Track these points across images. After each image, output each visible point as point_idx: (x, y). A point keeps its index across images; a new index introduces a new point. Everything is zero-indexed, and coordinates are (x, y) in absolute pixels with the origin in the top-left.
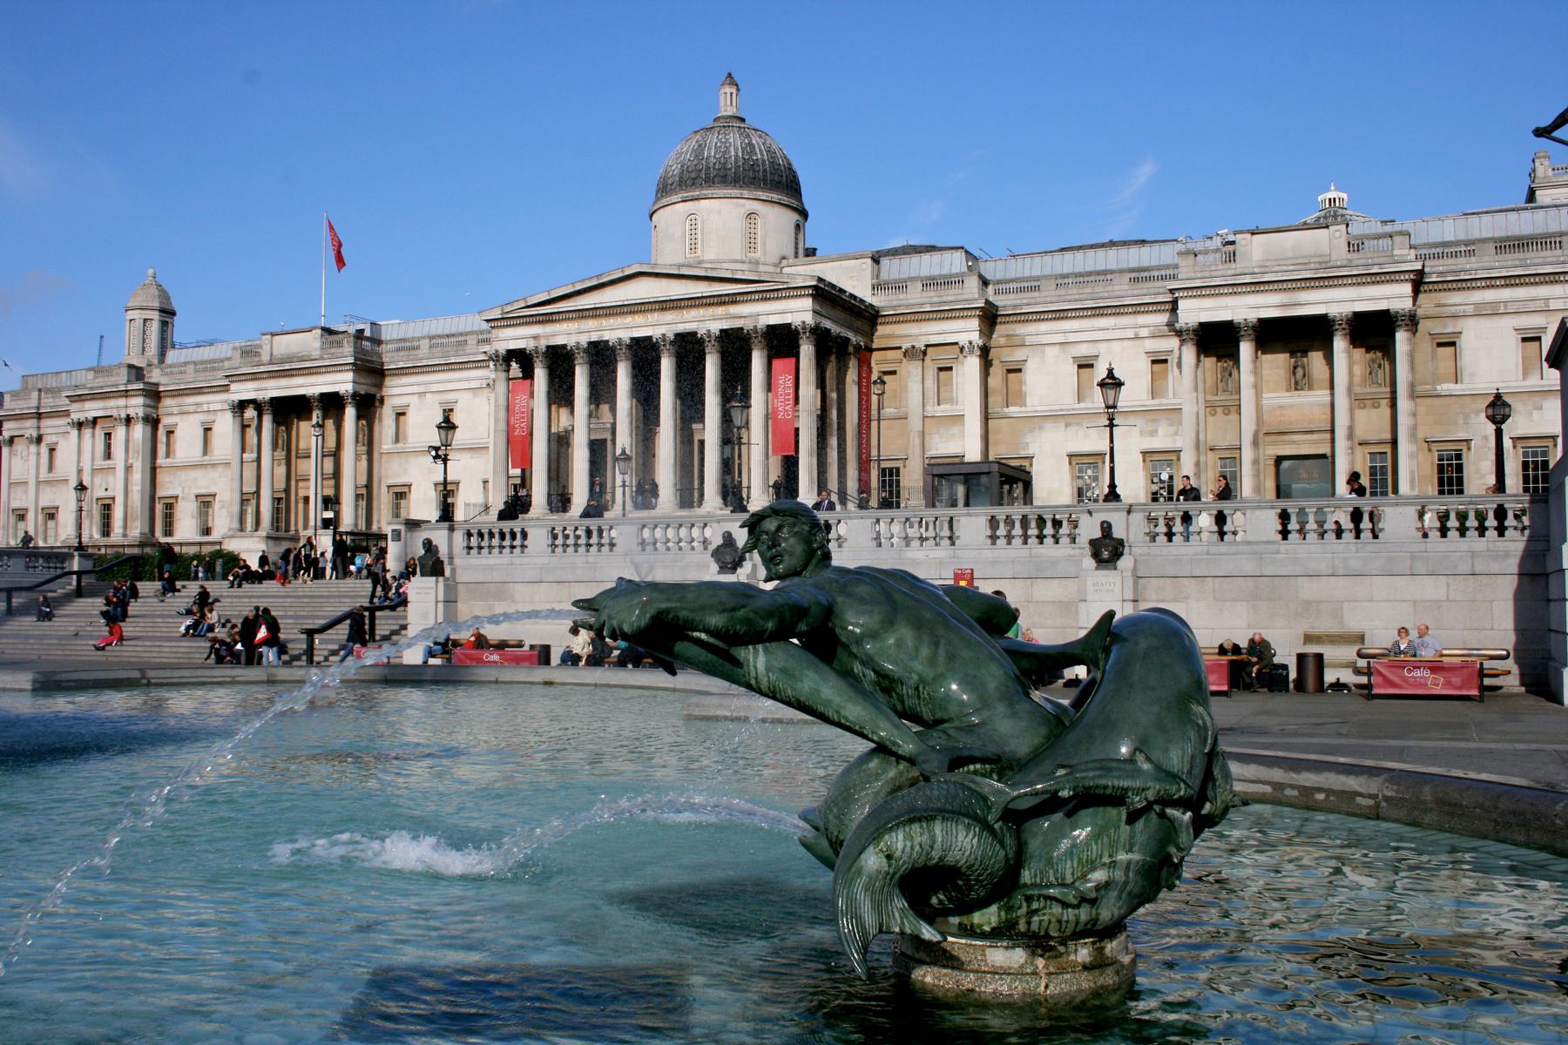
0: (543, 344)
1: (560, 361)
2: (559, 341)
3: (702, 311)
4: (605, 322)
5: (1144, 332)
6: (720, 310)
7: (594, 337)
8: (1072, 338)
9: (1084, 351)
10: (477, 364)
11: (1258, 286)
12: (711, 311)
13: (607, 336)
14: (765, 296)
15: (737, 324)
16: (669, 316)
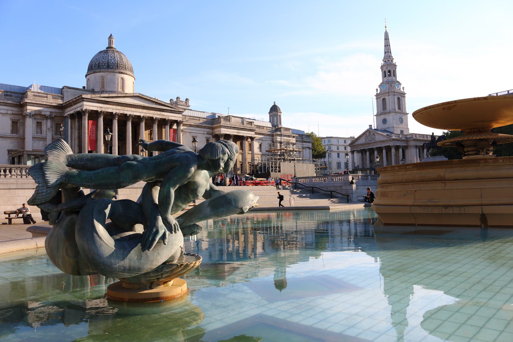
0: (103, 110)
1: (109, 118)
2: (110, 111)
3: (154, 112)
4: (126, 108)
5: (205, 133)
6: (159, 112)
7: (121, 112)
8: (192, 131)
9: (194, 135)
10: (6, 104)
11: (234, 128)
12: (156, 112)
13: (125, 112)
14: (171, 112)
15: (164, 117)
16: (145, 111)
